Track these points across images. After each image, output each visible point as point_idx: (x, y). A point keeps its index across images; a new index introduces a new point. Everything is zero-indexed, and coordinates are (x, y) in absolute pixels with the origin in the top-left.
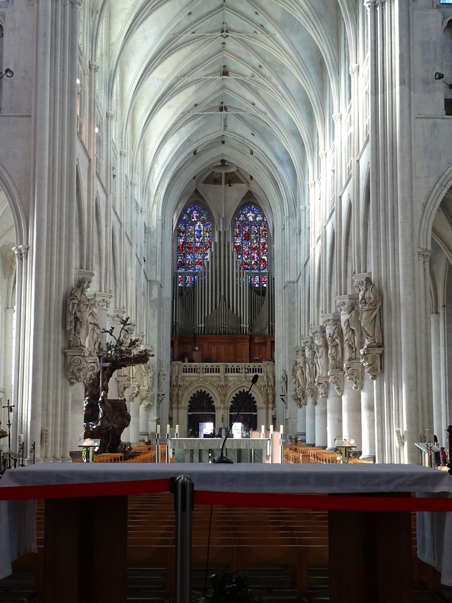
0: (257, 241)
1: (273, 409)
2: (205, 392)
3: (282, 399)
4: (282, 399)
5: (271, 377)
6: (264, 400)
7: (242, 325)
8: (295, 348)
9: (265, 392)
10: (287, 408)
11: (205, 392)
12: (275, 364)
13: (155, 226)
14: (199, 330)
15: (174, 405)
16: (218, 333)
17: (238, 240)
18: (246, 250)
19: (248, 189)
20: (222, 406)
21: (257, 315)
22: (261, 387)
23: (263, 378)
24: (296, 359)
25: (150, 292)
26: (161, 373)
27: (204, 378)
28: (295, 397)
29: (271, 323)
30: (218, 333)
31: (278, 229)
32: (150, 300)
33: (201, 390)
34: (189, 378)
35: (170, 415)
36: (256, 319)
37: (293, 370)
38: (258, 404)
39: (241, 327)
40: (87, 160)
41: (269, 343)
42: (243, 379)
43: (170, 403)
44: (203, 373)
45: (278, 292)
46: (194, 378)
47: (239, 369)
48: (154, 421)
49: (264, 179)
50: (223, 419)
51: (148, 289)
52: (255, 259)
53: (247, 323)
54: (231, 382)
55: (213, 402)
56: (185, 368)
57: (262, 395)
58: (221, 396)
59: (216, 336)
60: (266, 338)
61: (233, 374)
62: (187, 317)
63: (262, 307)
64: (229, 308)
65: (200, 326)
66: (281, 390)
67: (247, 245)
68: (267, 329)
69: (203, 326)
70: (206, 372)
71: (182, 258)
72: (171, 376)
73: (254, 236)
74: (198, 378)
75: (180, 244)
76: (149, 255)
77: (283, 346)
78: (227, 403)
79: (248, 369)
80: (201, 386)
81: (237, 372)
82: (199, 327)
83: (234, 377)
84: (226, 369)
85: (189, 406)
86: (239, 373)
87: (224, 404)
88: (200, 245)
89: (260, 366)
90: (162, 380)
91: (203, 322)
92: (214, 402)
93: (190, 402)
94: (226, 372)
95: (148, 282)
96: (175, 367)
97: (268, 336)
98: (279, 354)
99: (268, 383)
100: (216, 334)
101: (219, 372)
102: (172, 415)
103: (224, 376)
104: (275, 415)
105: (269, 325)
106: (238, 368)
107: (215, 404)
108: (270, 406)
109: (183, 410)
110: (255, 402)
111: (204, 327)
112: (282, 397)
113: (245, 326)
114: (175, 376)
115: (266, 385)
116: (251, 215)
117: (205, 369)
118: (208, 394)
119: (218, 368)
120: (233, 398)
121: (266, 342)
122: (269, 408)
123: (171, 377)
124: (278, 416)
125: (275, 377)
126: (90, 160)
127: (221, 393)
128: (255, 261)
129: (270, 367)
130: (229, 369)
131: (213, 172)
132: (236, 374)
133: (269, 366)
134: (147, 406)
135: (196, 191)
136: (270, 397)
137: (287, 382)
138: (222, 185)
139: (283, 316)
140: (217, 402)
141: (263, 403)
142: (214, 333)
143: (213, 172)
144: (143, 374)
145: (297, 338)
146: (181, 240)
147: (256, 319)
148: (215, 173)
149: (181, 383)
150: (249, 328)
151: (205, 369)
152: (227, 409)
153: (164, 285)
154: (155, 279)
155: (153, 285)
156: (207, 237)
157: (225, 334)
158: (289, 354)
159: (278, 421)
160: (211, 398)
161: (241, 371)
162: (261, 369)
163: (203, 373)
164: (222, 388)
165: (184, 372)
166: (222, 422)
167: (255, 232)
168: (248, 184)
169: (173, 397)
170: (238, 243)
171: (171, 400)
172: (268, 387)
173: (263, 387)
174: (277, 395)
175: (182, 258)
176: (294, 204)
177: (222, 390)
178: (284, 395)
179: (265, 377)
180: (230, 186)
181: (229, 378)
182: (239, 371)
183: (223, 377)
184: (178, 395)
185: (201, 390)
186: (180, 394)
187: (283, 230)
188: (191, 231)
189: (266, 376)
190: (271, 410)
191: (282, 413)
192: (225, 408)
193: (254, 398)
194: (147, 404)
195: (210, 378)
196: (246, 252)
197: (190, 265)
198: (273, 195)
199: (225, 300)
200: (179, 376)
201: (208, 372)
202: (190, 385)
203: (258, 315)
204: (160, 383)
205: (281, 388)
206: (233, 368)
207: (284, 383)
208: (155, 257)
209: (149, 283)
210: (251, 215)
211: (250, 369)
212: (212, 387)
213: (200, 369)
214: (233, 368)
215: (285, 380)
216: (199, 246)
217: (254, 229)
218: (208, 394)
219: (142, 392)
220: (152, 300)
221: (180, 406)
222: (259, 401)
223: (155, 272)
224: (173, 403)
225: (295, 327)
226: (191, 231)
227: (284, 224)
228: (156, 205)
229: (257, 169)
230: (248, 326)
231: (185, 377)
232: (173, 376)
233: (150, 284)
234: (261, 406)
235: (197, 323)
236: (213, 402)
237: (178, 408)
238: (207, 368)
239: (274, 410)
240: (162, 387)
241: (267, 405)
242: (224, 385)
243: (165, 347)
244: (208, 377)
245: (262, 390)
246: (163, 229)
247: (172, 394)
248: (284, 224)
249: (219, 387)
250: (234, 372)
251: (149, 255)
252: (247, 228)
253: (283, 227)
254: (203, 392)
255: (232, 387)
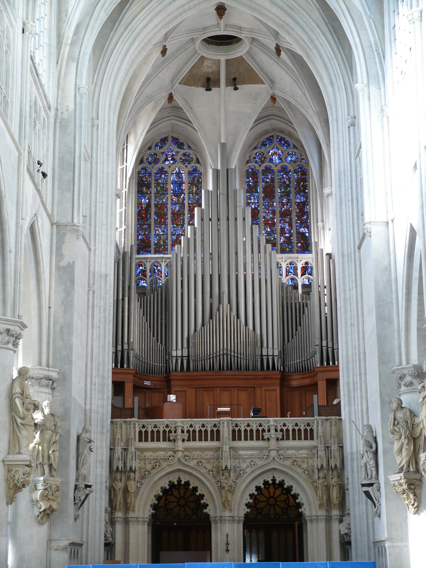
0: (289, 200)
1: (341, 521)
2: (187, 483)
3: (367, 494)
4: (367, 494)
5: (334, 447)
6: (321, 500)
7: (265, 353)
8: (393, 372)
9: (321, 481)
10: (379, 516)
11: (187, 483)
12: (341, 420)
13: (71, 107)
14: (177, 360)
15: (119, 514)
16: (216, 367)
17: (252, 198)
18: (268, 217)
19: (271, 92)
20: (227, 514)
21: (294, 331)
22: (313, 472)
23: (316, 451)
24: (398, 396)
25: (59, 249)
26: (84, 435)
27: (186, 453)
28: (401, 485)
29: (324, 343)
30: (216, 367)
31: (340, 128)
32: (58, 268)
33: (179, 481)
34: (151, 453)
35: (109, 535)
36: (292, 338)
37: (395, 419)
38: (306, 510)
39: (262, 355)
40: (17, 154)
41: (322, 386)
42: (273, 454)
43: (109, 509)
44: (183, 440)
45: (346, 258)
46: (163, 453)
47: (263, 431)
48: (65, 549)
49: (308, 29)
50: (227, 544)
51: (54, 242)
52: (286, 233)
53: (276, 346)
54: (244, 460)
55: (206, 506)
56: (143, 430)
57: (316, 488)
58: (223, 492)
59: (211, 373)
60: (316, 375)
61: (249, 443)
62: (153, 336)
63: (304, 313)
64: (238, 317)
65: (179, 354)
66: (364, 473)
67: (270, 208)
68: (318, 356)
69: (185, 354)
70: (189, 440)
71: (145, 234)
72: (111, 449)
73: (283, 190)
74: (170, 453)
75: (142, 207)
76: (57, 169)
77: (360, 374)
78: (239, 509)
79: (282, 430)
80: (179, 470)
81: (258, 439)
82: (177, 357)
83: (252, 449)
84: (234, 431)
85: (153, 516)
86: (263, 439)
87: (231, 510)
88: (180, 207)
89: (308, 425)
90: (86, 451)
91: (185, 345)
92: (207, 505)
93: (155, 507)
94: (234, 439)
95: (55, 226)
96: (121, 428)
97: (321, 369)
98: (352, 392)
99: (328, 461)
100: (212, 368)
101: (218, 439)
102: (113, 535)
103: (230, 448)
104: (346, 534)
105: (322, 347)
106: (260, 429)
107: (210, 510)
108: (335, 513)
109: (140, 526)
110: (299, 505)
111: (188, 356)
112: (366, 489)
113: (270, 353)
114: (120, 448)
115: (325, 466)
116: (275, 153)
117: (188, 431)
118: (195, 489)
119: (215, 429)
120: (251, 496)
121: (316, 384)
122: (333, 518)
123: (112, 450)
124: (356, 537)
125: (342, 447)
126: (20, 154)
127: (224, 485)
128: (286, 237)
129: (331, 426)
130: (240, 431)
131: (203, 58)
132: (255, 443)
133: (328, 424)
134: (44, 511)
135: (171, 98)
136: (335, 493)
137: (376, 453)
138: (219, 87)
139: (357, 310)
140: (215, 506)
141: (317, 507)
142: (207, 367)
143: (203, 58)
144: (19, 421)
145: (400, 348)
146: (143, 200)
147: (292, 338)
148: (206, 63)
149: (135, 464)
150: (279, 356)
151: (188, 431)
152: (239, 521)
153: (95, 245)
154: (71, 221)
155: (65, 234)
156: (193, 194)
157: (231, 369)
158: (381, 384)
159: (356, 548)
160: (202, 496)
161: (266, 436)
162: (312, 430)
163: (183, 440)
164: (226, 474)
165: (140, 440)
166: (227, 551)
167: (284, 182)
168: (272, 82)
169: (115, 496)
170: (253, 203)
171: (111, 502)
172: (328, 470)
173: (316, 471)
174: (350, 487)
175: (145, 234)
176: (379, 54)
177: (226, 478)
178: (371, 485)
179: (321, 448)
180: (236, 89)
181: (241, 452)
182: (263, 436)
183: (228, 449)
184: (126, 491)
185: (179, 481)
186: (132, 486)
187: (351, 128)
188: (163, 184)
189: (323, 446)
190: (337, 523)
191: (365, 530)
192: (233, 519)
193: (295, 497)
194: (43, 508)
195: (199, 453)
196: (268, 220)
197: (161, 246)
198: (326, 60)
199: (229, 302)
200: (130, 448)
201: (194, 440)
202: (153, 468)
203: (296, 330)
204: (81, 459)
205: (364, 468)
206: (249, 429)
207: (371, 456)
208: (71, 173)
209: (57, 230)
210: (275, 153)
211: (288, 430)
212: (204, 471)
213: (175, 432)
214: (249, 429)
215: (371, 447)
216: (179, 211)
217: (283, 178)
218: (195, 489)
219: (14, 469)
220: (64, 267)
221: (131, 515)
222: (309, 504)
223: (69, 205)
224: (115, 509)
225: (391, 322)
226: (163, 184)
227: (352, 114)
228: (75, 64)
229: (293, 10)
230: (276, 353)
231: (142, 450)
232: (117, 448)
233: (57, 233)
234: (314, 513)
235: (174, 348)
236: (206, 506)
237: (126, 522)
238: (191, 430)
239: (344, 523)
240: (85, 467)
241: (327, 510)
242: (229, 468)
243: (96, 380)
244: (195, 449)
245: (316, 477)
246: (95, 129)
247: (114, 489)
248: (352, 114)
249: (218, 472)
250: (252, 439)
251: (57, 169)
252: (269, 176)
253: (350, 120)
254: (183, 483)
255: (249, 470)
